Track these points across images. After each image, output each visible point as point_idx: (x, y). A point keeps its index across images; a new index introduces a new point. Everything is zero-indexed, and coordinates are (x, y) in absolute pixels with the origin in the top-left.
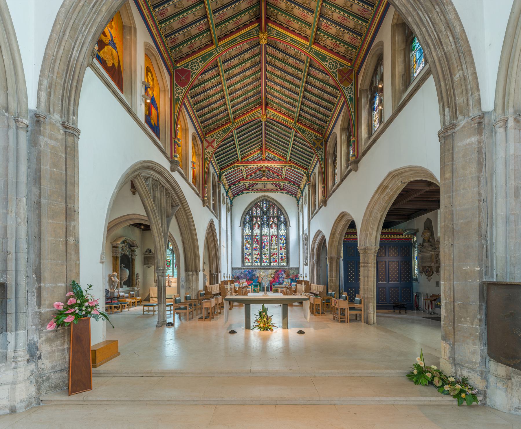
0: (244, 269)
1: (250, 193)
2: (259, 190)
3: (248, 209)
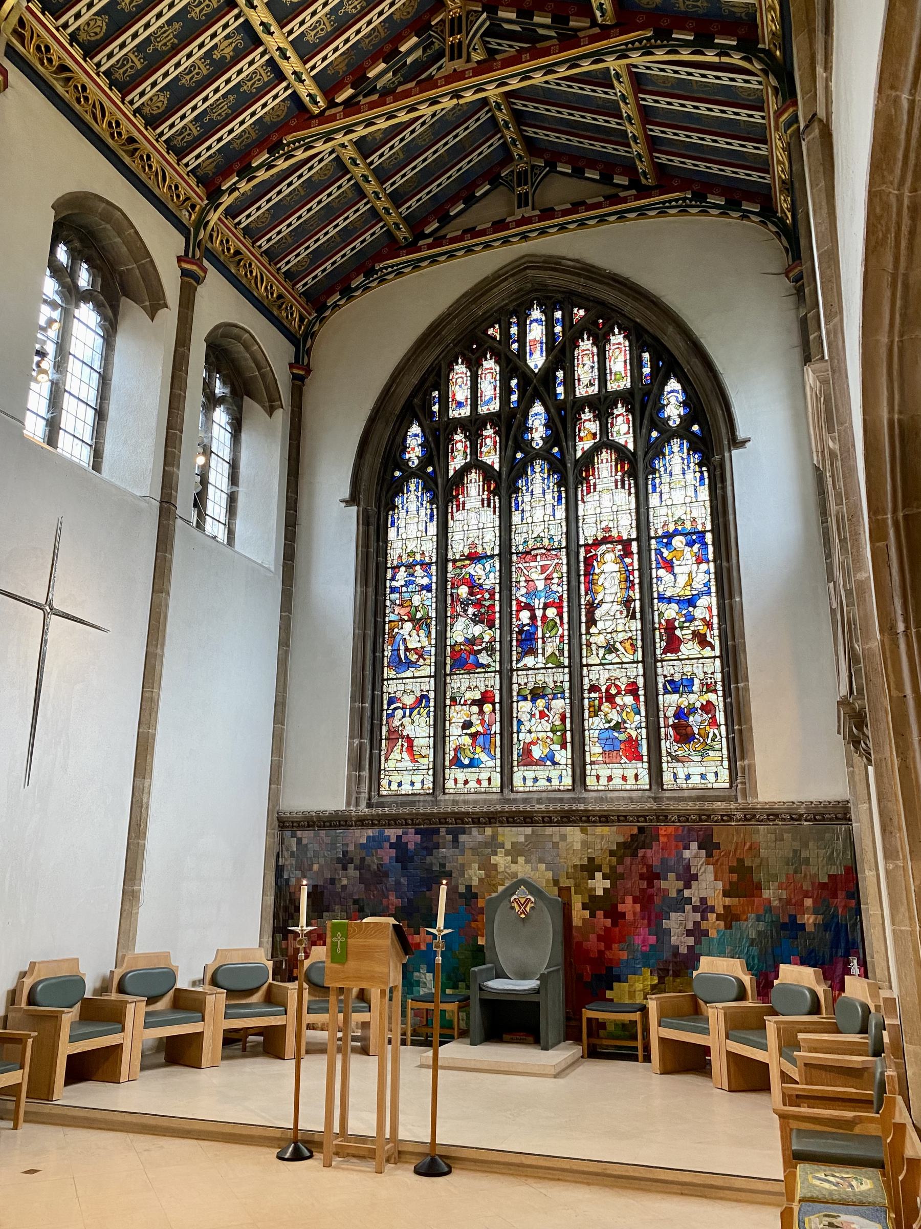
1: (428, 271)
2: (483, 233)
3: (413, 379)
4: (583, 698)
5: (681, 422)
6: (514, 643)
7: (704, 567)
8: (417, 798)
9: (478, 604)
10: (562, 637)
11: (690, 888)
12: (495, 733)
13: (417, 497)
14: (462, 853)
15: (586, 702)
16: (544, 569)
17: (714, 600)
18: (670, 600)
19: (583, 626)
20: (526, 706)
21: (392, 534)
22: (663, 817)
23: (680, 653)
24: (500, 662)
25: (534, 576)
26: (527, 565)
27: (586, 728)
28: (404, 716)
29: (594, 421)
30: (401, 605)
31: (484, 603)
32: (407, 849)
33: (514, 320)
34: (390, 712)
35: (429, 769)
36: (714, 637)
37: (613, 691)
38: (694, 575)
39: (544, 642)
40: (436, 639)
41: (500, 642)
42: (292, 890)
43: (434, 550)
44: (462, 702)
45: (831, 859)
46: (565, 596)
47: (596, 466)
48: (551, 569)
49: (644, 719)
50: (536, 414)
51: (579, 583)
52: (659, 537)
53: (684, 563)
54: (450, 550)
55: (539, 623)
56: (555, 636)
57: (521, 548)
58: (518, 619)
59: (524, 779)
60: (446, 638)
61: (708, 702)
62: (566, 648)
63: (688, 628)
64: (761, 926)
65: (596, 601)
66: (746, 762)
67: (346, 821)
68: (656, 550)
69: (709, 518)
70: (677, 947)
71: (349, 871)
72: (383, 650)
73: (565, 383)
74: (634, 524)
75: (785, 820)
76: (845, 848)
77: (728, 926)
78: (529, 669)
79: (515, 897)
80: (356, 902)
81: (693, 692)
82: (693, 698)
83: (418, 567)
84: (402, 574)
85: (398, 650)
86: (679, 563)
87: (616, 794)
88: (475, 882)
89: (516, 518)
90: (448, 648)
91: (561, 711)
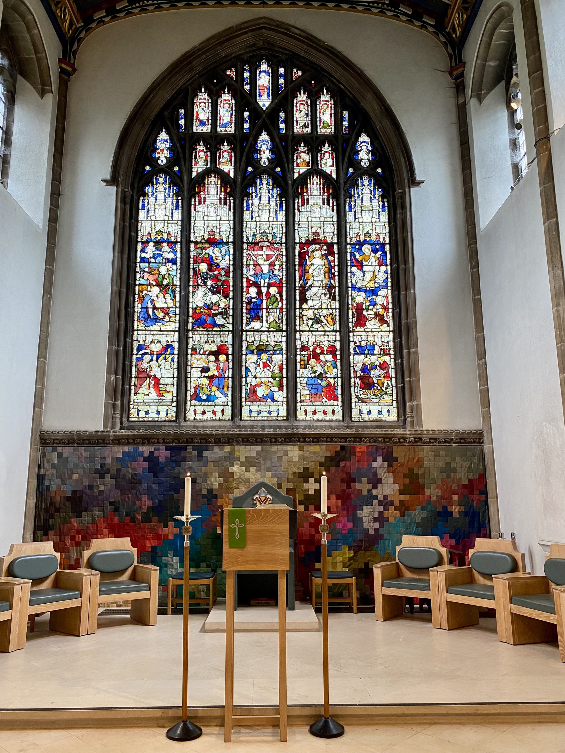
0: (118, 441)
3: (165, 95)
4: (296, 355)
5: (370, 164)
6: (244, 311)
7: (383, 268)
8: (163, 423)
9: (216, 278)
10: (281, 309)
11: (376, 488)
12: (228, 377)
13: (165, 189)
14: (206, 465)
15: (298, 358)
16: (268, 257)
17: (390, 292)
18: (360, 289)
19: (297, 303)
20: (253, 358)
21: (142, 215)
22: (358, 438)
23: (366, 327)
24: (233, 324)
25: (261, 262)
26: (256, 253)
27: (298, 376)
28: (151, 360)
29: (308, 153)
30: (150, 273)
31: (220, 278)
32: (158, 462)
33: (247, 67)
34: (139, 356)
35: (172, 402)
37: (318, 351)
38: (377, 273)
39: (267, 312)
40: (180, 302)
41: (233, 309)
42: (53, 495)
43: (179, 232)
44: (202, 352)
45: (470, 469)
46: (284, 279)
47: (309, 186)
48: (274, 258)
49: (339, 372)
50: (263, 141)
51: (295, 270)
52: (353, 244)
53: (370, 264)
54: (192, 234)
55: (264, 297)
56: (276, 308)
57: (250, 239)
58: (248, 293)
59: (251, 411)
60: (188, 302)
61: (384, 362)
62: (284, 317)
63: (372, 310)
64: (424, 514)
65: (307, 285)
66: (415, 403)
67: (104, 440)
68: (351, 252)
69: (388, 234)
70: (368, 530)
71: (106, 479)
72: (134, 307)
73: (285, 121)
74: (335, 233)
75: (440, 442)
76: (479, 461)
77: (403, 515)
78: (255, 331)
79: (257, 496)
80: (111, 504)
81: (374, 355)
82: (373, 358)
83: (165, 244)
84: (151, 248)
85: (147, 308)
86: (366, 263)
87: (319, 424)
88: (215, 486)
89: (247, 216)
90: (191, 310)
91: (280, 363)
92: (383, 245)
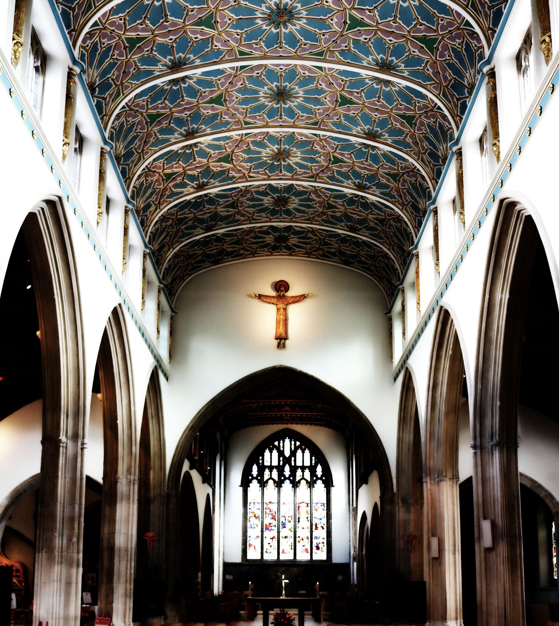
9: (272, 514)
36: (325, 527)
92: (324, 504)
